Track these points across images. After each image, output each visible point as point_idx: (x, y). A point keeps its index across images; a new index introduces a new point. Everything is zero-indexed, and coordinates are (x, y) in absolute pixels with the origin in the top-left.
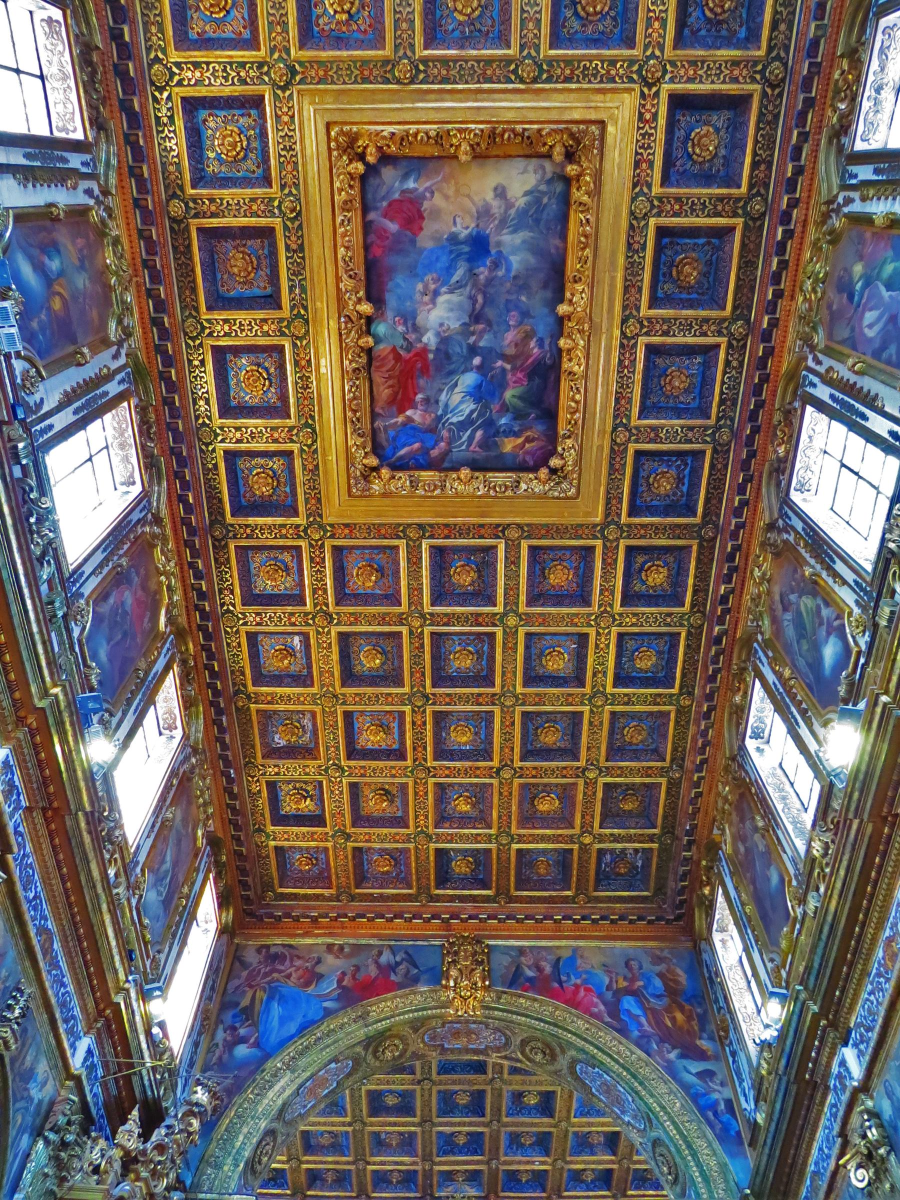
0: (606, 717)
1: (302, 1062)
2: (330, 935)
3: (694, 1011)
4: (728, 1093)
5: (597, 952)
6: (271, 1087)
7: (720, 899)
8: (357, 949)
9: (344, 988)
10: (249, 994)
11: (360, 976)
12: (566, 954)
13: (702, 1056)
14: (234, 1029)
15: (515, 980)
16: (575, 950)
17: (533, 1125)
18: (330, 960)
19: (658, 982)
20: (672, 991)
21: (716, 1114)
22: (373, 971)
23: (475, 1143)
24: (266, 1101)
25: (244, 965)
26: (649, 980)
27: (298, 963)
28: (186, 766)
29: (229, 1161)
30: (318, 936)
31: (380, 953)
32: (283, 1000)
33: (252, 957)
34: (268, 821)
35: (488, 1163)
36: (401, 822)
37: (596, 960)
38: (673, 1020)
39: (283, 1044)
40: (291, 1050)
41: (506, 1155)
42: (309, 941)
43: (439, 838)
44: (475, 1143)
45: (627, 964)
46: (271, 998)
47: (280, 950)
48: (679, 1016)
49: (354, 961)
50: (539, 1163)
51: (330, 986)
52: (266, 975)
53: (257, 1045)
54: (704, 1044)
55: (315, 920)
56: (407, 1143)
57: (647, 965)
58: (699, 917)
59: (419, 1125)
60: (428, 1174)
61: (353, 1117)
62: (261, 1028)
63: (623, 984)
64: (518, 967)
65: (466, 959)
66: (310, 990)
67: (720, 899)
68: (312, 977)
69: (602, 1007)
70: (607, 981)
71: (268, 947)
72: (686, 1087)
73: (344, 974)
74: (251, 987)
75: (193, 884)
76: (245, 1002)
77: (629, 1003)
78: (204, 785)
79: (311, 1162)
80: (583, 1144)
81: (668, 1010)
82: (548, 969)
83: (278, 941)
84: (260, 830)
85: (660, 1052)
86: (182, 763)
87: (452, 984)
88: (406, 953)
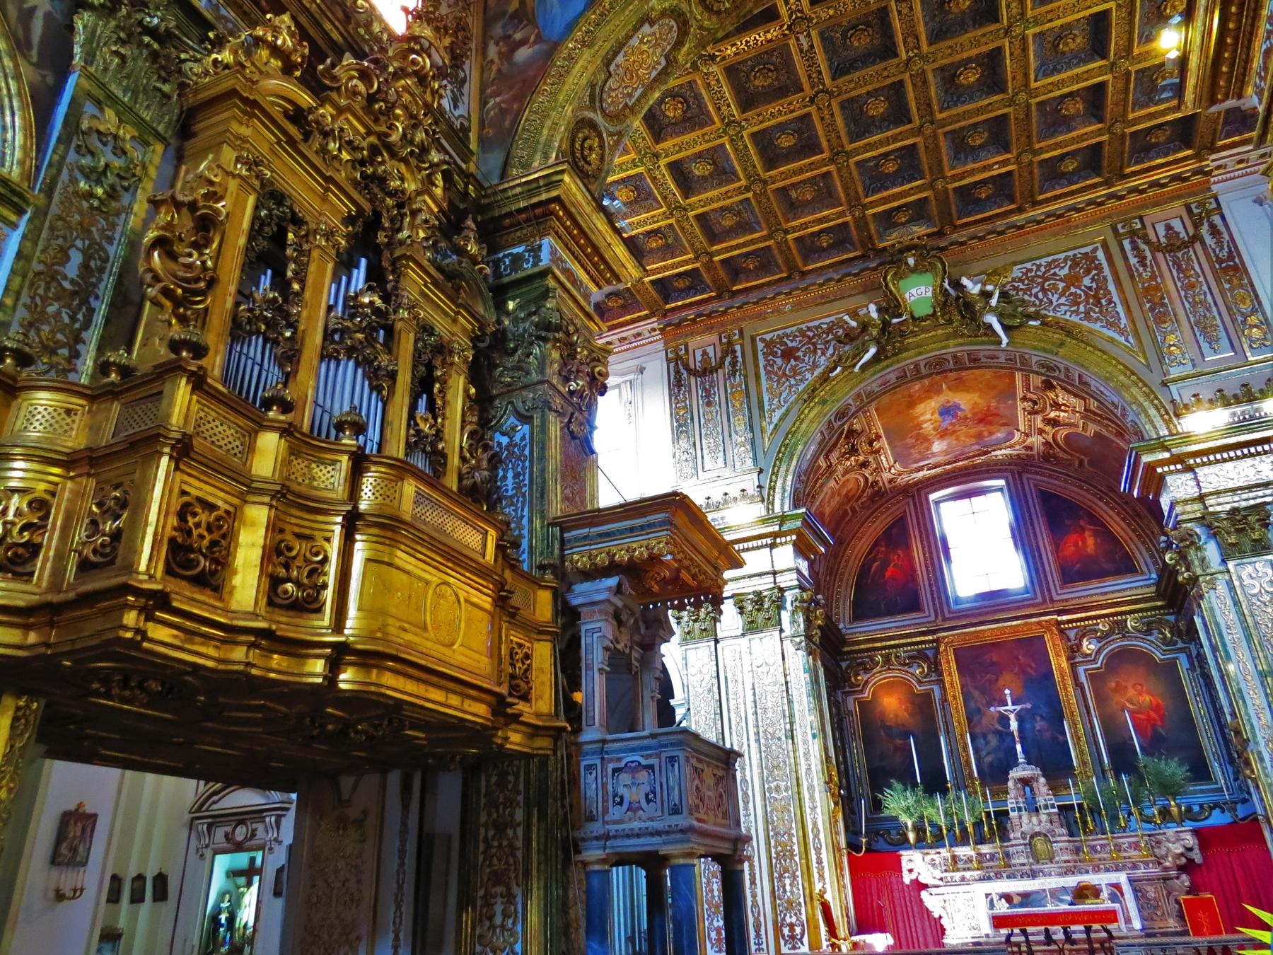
17: (979, 111)
23: (909, 164)
24: (566, 87)
29: (538, 157)
35: (931, 186)
39: (570, 28)
41: (953, 168)
44: (909, 164)
50: (995, 164)
53: (539, 39)
56: (825, 195)
59: (832, 161)
60: (862, 223)
61: (748, 177)
62: (540, 22)
79: (722, 251)
80: (1054, 117)
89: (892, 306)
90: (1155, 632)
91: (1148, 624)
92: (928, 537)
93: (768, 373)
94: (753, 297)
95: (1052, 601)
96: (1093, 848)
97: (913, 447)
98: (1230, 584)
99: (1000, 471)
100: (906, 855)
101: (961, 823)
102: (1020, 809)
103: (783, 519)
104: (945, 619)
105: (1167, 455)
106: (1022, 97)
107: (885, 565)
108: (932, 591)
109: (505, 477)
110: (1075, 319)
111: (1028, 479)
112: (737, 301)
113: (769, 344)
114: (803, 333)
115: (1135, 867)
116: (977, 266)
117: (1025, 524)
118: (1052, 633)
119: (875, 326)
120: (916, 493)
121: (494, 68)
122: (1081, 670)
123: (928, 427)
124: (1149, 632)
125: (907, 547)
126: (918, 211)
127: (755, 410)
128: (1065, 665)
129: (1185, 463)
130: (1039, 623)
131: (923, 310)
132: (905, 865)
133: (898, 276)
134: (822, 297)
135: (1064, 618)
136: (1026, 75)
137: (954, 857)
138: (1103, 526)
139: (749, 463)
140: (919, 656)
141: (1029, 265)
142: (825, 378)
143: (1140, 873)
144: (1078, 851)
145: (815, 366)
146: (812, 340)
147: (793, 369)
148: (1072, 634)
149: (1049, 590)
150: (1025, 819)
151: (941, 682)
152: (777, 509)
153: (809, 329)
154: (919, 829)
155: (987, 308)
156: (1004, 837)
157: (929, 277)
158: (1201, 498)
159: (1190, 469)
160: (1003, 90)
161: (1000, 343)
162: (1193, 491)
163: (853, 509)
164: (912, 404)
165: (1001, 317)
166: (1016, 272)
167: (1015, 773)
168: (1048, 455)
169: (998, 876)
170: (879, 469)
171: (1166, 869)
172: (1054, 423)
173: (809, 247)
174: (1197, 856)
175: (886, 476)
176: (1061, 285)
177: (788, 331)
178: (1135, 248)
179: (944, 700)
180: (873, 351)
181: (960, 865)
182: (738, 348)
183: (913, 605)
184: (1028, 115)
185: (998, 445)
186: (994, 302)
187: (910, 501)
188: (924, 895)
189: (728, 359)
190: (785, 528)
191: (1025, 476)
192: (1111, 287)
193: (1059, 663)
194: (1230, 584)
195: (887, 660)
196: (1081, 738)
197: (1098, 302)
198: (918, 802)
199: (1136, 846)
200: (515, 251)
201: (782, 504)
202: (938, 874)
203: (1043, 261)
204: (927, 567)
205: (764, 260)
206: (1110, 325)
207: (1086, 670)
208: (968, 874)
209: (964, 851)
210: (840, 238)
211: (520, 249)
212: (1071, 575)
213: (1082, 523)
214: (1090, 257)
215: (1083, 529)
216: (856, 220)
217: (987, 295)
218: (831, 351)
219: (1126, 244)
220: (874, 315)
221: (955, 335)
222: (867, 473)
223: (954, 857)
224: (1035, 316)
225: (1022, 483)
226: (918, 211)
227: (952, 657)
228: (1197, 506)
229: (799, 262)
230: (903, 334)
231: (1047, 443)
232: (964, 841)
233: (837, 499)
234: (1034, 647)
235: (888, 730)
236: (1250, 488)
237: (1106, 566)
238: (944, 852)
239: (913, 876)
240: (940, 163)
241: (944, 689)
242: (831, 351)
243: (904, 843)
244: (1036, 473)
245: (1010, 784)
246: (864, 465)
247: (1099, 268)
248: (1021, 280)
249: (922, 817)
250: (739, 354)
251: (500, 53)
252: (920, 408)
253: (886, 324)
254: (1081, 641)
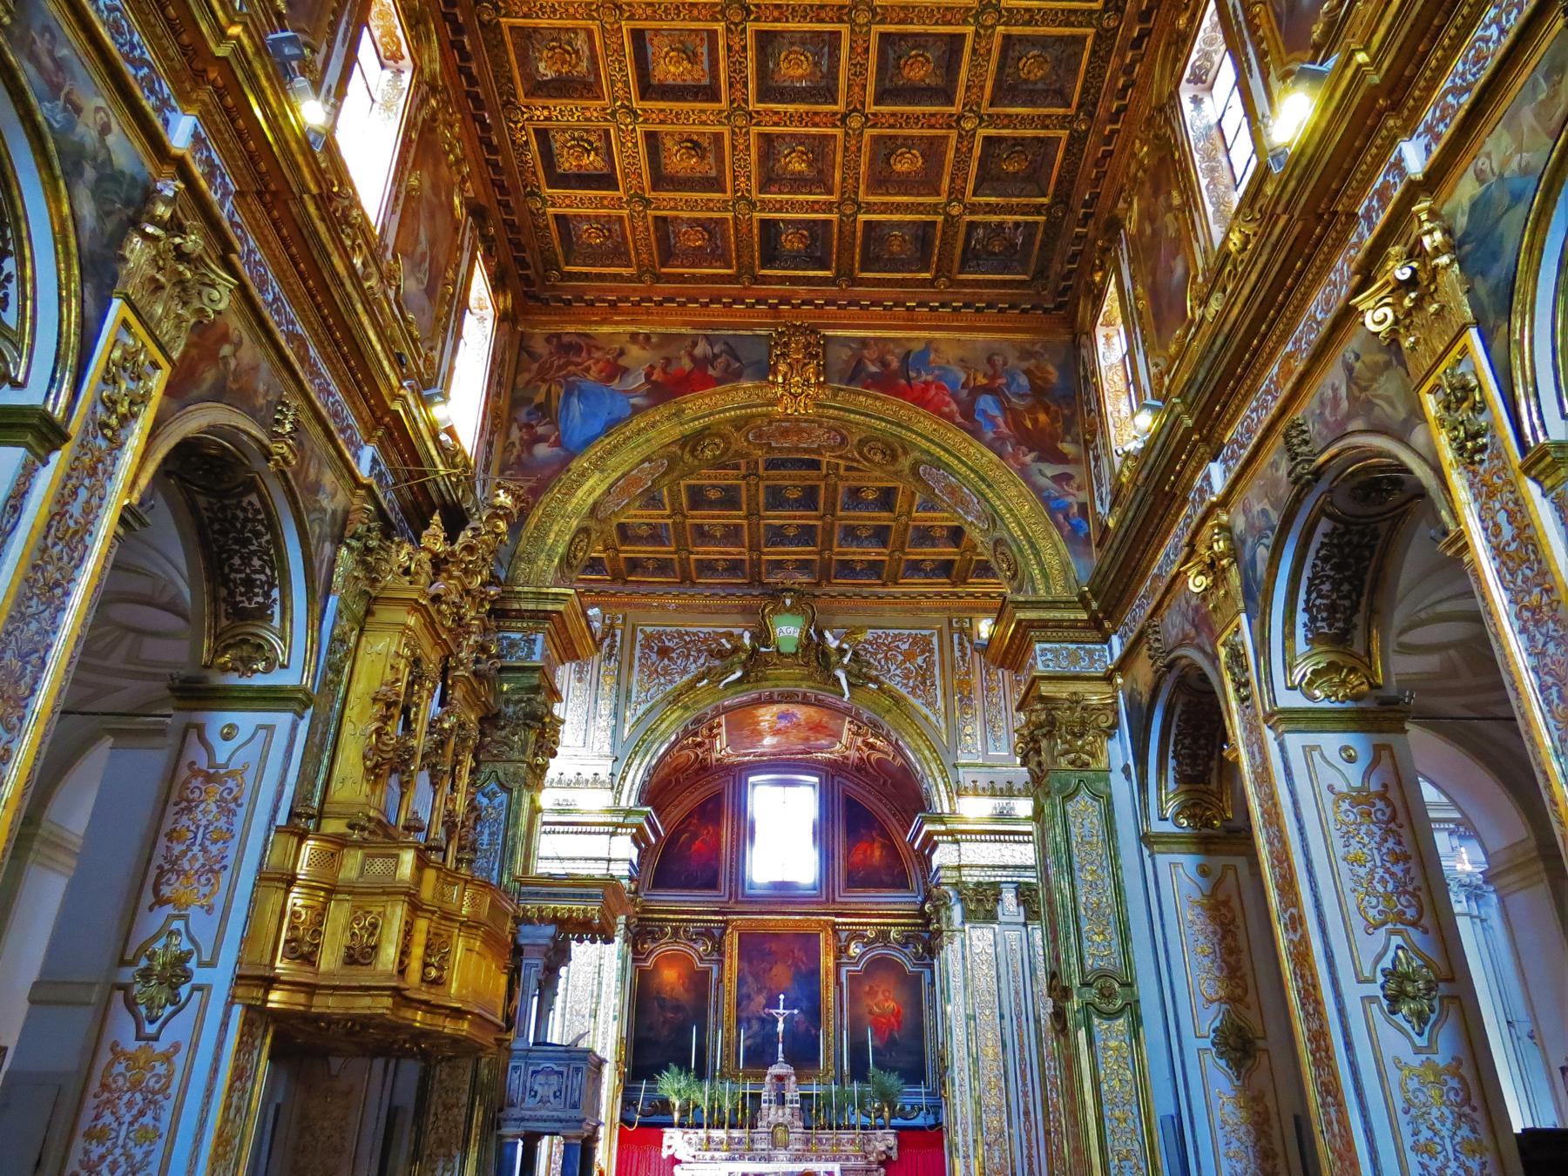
0: (997, 42)
1: (612, 462)
2: (632, 322)
3: (1059, 410)
4: (1083, 496)
5: (953, 345)
6: (579, 487)
7: (1112, 288)
8: (667, 339)
9: (654, 383)
10: (544, 388)
11: (671, 369)
12: (918, 347)
13: (1062, 458)
14: (530, 427)
15: (855, 375)
16: (930, 342)
18: (635, 351)
19: (1023, 381)
20: (1039, 391)
21: (1066, 517)
22: (687, 364)
24: (575, 500)
25: (532, 356)
26: (1013, 378)
27: (597, 355)
28: (424, 113)
29: (543, 556)
30: (617, 323)
31: (695, 344)
32: (582, 396)
33: (541, 348)
34: (543, 182)
36: (715, 184)
37: (952, 353)
38: (1035, 421)
39: (588, 442)
40: (596, 450)
42: (606, 329)
43: (765, 205)
45: (990, 360)
46: (568, 394)
47: (576, 339)
48: (1042, 417)
49: (664, 353)
51: (637, 381)
52: (560, 368)
53: (558, 443)
54: (1067, 448)
55: (613, 304)
57: (1012, 361)
58: (1083, 308)
60: (756, 564)
62: (561, 426)
63: (982, 380)
64: (860, 362)
65: (797, 351)
66: (615, 384)
67: (1112, 288)
68: (615, 370)
69: (954, 407)
70: (963, 377)
71: (559, 336)
72: (1038, 490)
73: (652, 367)
74: (544, 381)
75: (458, 265)
76: (540, 397)
77: (986, 403)
78: (449, 135)
81: (1031, 410)
82: (895, 364)
83: (571, 329)
84: (532, 194)
85: (1015, 456)
86: (419, 109)
87: (780, 379)
88: (726, 343)
89: (762, 635)
91: (907, 937)
93: (641, 665)
94: (643, 589)
95: (834, 901)
96: (820, 1140)
98: (963, 941)
100: (668, 1132)
101: (720, 1108)
103: (628, 813)
104: (737, 902)
105: (943, 828)
106: (904, 519)
107: (694, 836)
109: (482, 832)
110: (904, 691)
112: (629, 589)
113: (648, 638)
114: (680, 635)
115: (848, 1159)
116: (840, 619)
119: (745, 651)
120: (737, 775)
121: (515, 452)
122: (844, 970)
123: (764, 725)
124: (905, 945)
125: (718, 824)
126: (804, 566)
127: (623, 696)
128: (831, 965)
129: (955, 837)
131: (788, 648)
132: (666, 1141)
133: (774, 611)
134: (705, 606)
135: (840, 920)
136: (911, 506)
137: (708, 1138)
138: (890, 840)
139: (607, 749)
140: (707, 934)
141: (880, 632)
142: (691, 686)
143: (850, 1164)
144: (807, 1141)
145: (685, 671)
146: (691, 645)
147: (665, 668)
148: (843, 935)
150: (773, 1111)
151: (721, 962)
152: (623, 804)
153: (687, 633)
154: (684, 1112)
155: (839, 664)
156: (753, 1126)
157: (800, 620)
158: (959, 868)
159: (957, 842)
160: (891, 511)
161: (843, 695)
162: (954, 861)
163: (677, 780)
165: (848, 673)
166: (869, 635)
167: (775, 1070)
168: (861, 767)
169: (742, 1157)
170: (712, 748)
171: (870, 1163)
172: (872, 747)
173: (706, 567)
174: (894, 1155)
175: (715, 755)
176: (900, 658)
177: (668, 630)
178: (961, 644)
179: (720, 980)
180: (739, 674)
181: (712, 1146)
182: (618, 632)
183: (712, 884)
184: (906, 530)
185: (821, 749)
186: (846, 660)
188: (677, 1169)
189: (607, 641)
190: (628, 821)
191: (837, 779)
192: (937, 671)
193: (827, 961)
194: (963, 941)
195: (676, 931)
196: (832, 1042)
197: (924, 682)
198: (689, 1085)
199: (852, 1142)
200: (513, 636)
201: (629, 799)
202: (692, 1152)
203: (891, 632)
205: (663, 567)
206: (928, 705)
208: (717, 1155)
209: (719, 1134)
210: (734, 567)
211: (518, 636)
212: (853, 882)
214: (927, 641)
215: (874, 841)
216: (751, 559)
217: (841, 652)
218: (702, 661)
219: (956, 637)
220: (747, 641)
221: (809, 677)
222: (699, 751)
223: (708, 1138)
224: (876, 680)
226: (804, 566)
227: (736, 940)
228: (955, 873)
229: (694, 575)
230: (766, 664)
231: (861, 759)
232: (721, 1126)
234: (808, 942)
235: (662, 1003)
236: (993, 867)
237: (885, 878)
238: (702, 1133)
239: (671, 1152)
240: (831, 540)
241: (721, 969)
242: (702, 661)
243: (671, 1125)
245: (768, 1078)
246: (700, 745)
247: (931, 651)
248: (871, 643)
249: (688, 1100)
250: (618, 639)
251: (521, 439)
253: (754, 651)
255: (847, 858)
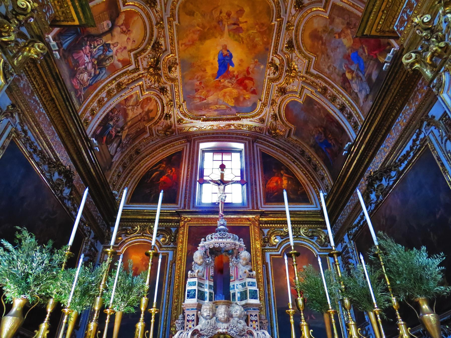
90: (316, 238)
92: (193, 163)
97: (197, 90)
99: (242, 139)
102: (201, 296)
108: (186, 193)
111: (257, 146)
117: (251, 167)
118: (255, 225)
122: (268, 255)
124: (312, 237)
125: (178, 166)
130: (248, 219)
135: (264, 219)
138: (293, 175)
148: (266, 231)
149: (257, 204)
151: (175, 249)
163: (150, 129)
164: (203, 37)
172: (283, 91)
187: (188, 144)
191: (255, 144)
204: (187, 179)
207: (271, 255)
213: (282, 172)
215: (282, 175)
225: (253, 147)
231: (275, 117)
233: (140, 111)
241: (175, 254)
244: (262, 143)
252: (208, 43)
254: (271, 236)
255: (265, 185)
